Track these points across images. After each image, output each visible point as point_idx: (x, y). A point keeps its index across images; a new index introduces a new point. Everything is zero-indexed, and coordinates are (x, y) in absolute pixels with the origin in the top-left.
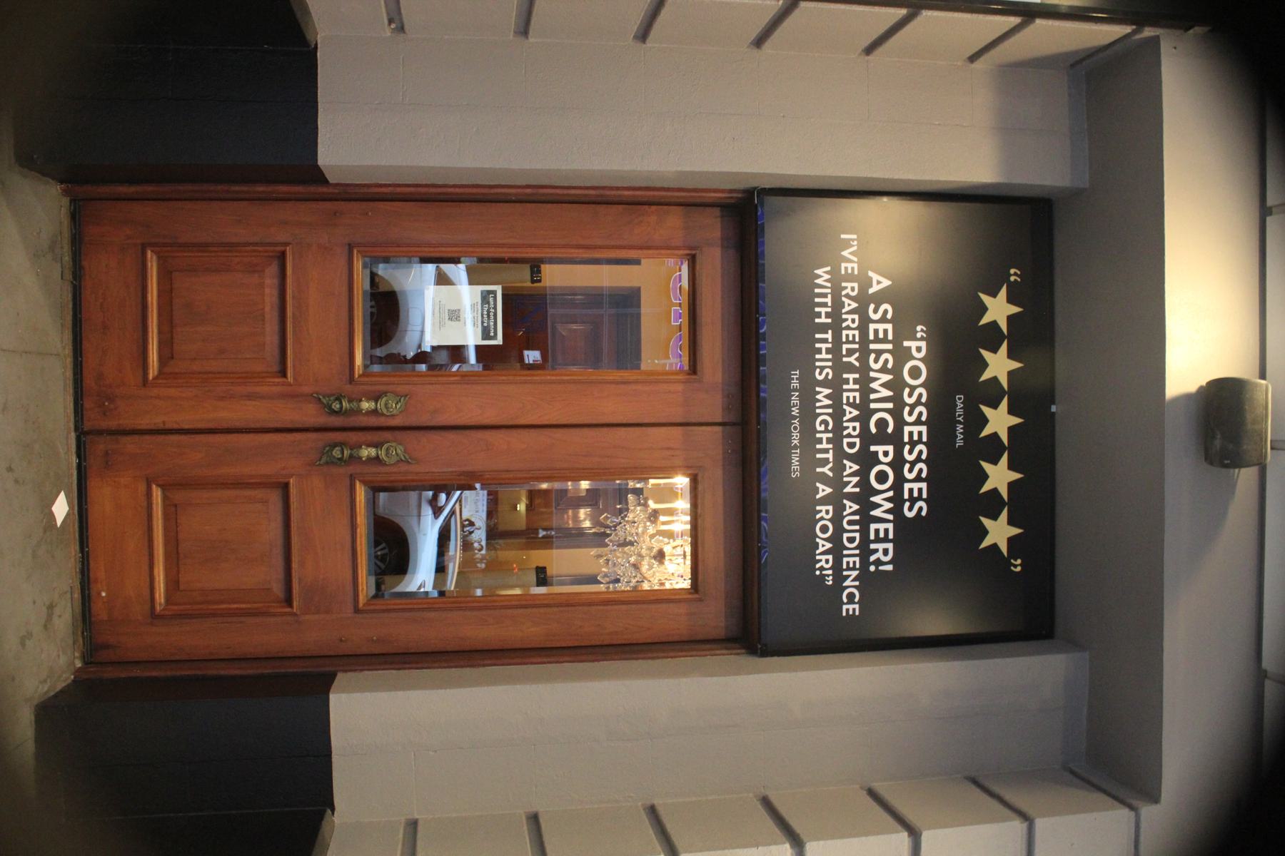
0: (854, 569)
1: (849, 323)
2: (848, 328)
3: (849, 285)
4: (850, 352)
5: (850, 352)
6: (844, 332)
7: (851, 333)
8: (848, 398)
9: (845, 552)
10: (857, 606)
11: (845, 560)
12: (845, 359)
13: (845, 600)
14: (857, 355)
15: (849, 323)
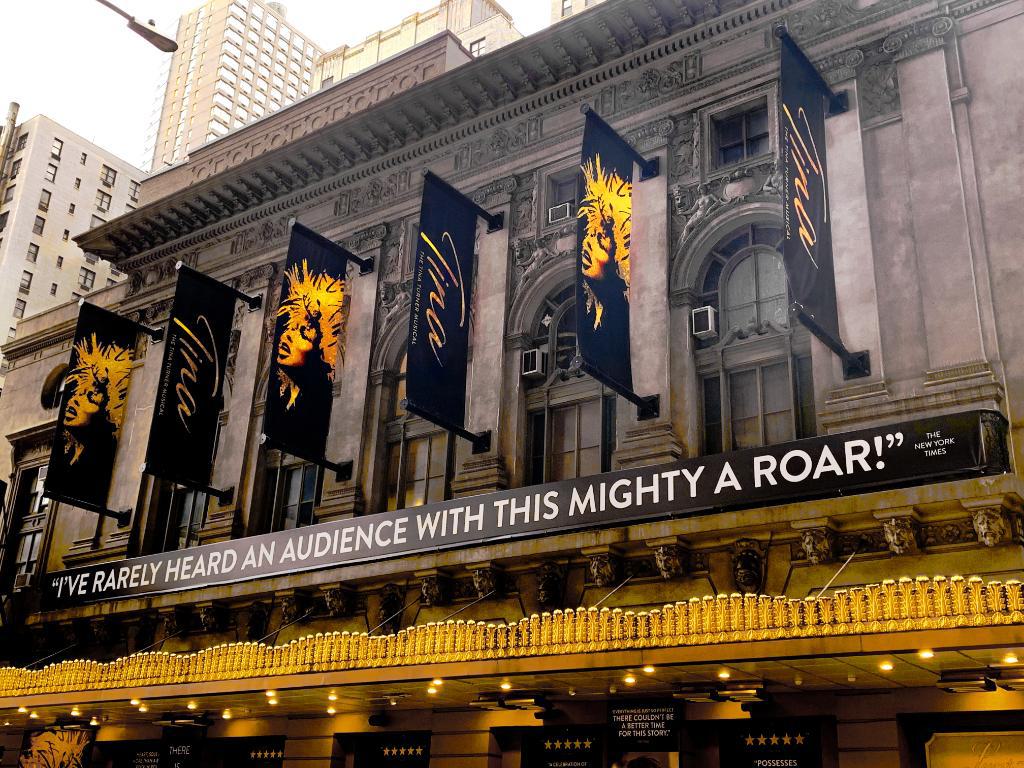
0: (353, 535)
3: (96, 582)
9: (334, 552)
10: (399, 521)
11: (343, 550)
12: (153, 582)
13: (389, 541)
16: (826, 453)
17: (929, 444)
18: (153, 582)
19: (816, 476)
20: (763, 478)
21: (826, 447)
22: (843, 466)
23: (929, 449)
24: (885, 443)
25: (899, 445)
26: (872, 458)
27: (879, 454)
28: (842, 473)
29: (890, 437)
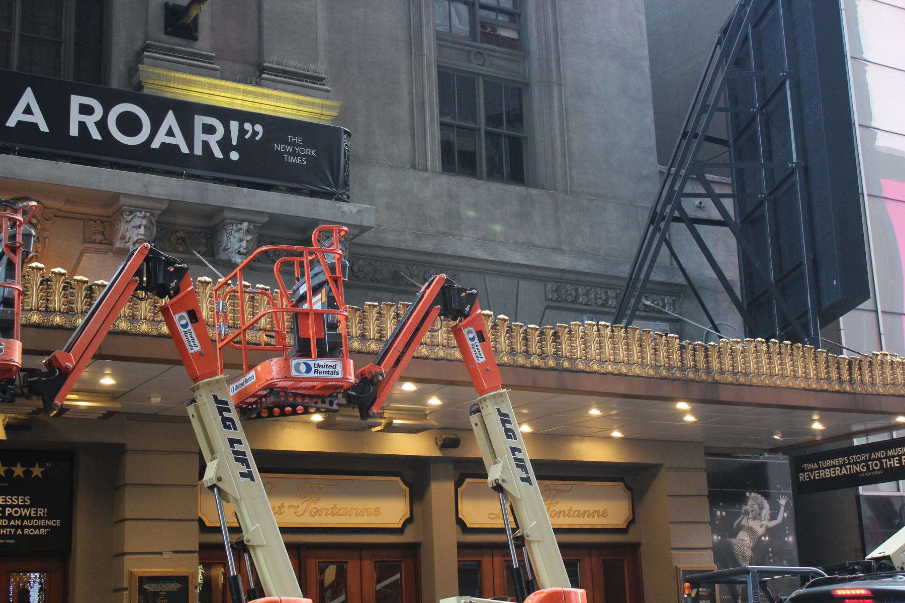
16: (170, 120)
17: (289, 149)
19: (155, 145)
20: (82, 126)
21: (171, 113)
22: (190, 142)
23: (288, 153)
24: (242, 132)
25: (257, 138)
26: (225, 144)
27: (234, 142)
28: (188, 152)
29: (248, 126)
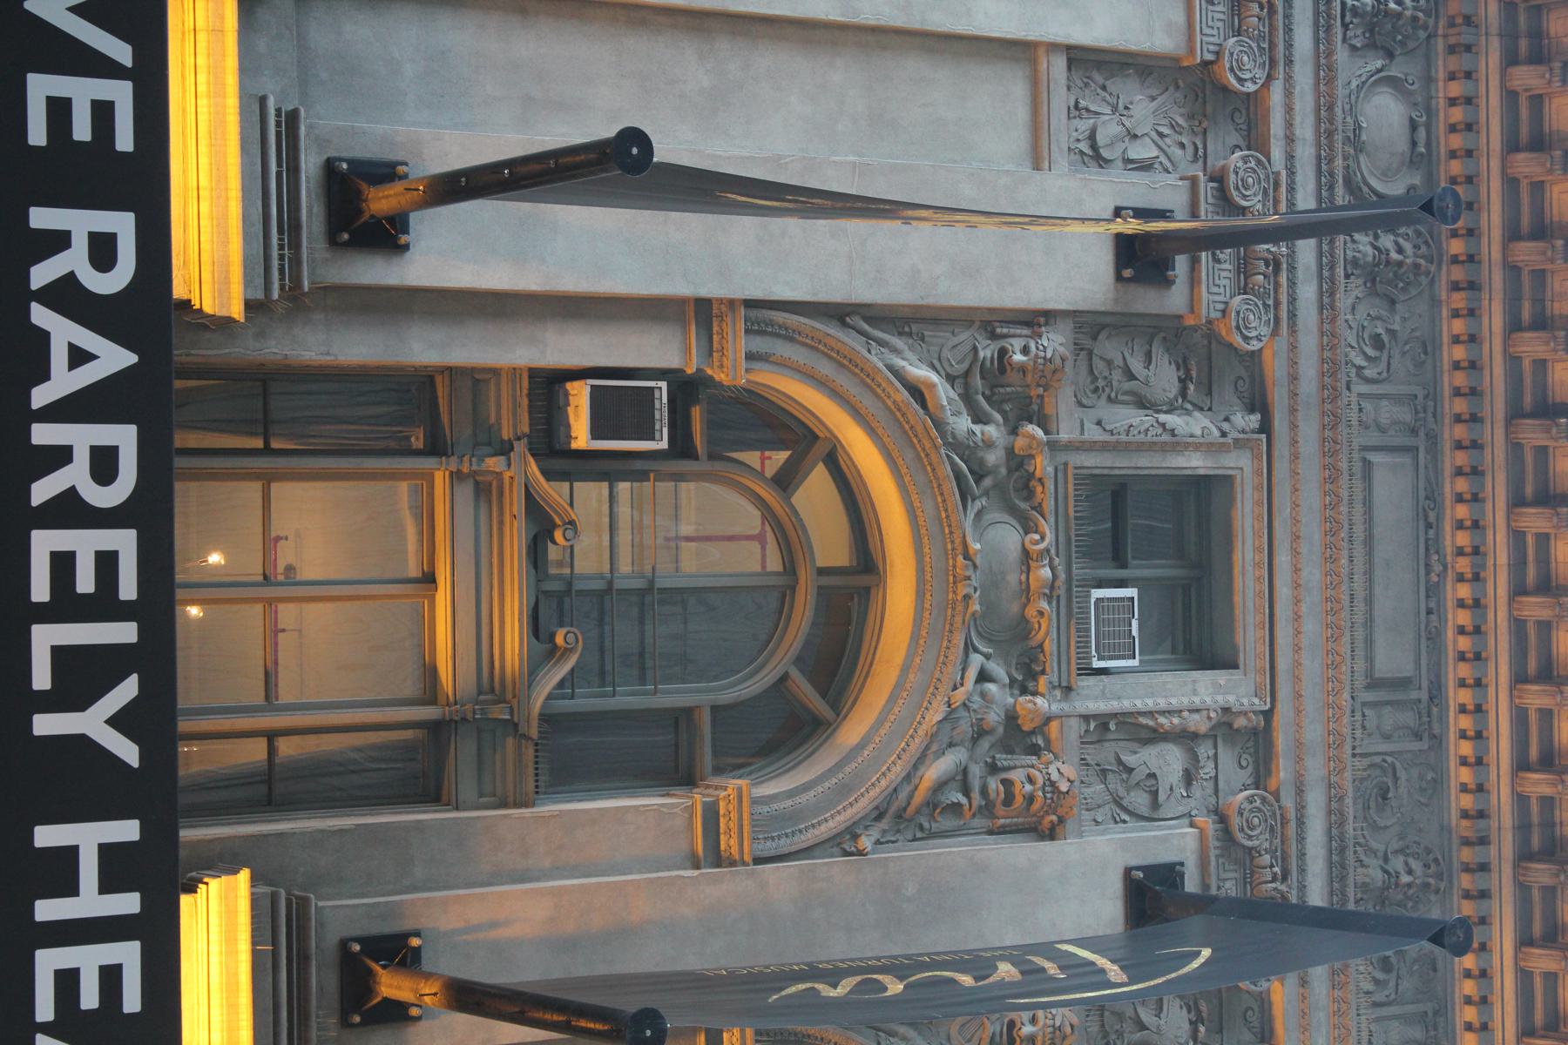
1: (76, 475)
2: (70, 512)
3: (80, 222)
4: (82, 676)
5: (82, 676)
6: (44, 543)
7: (85, 543)
8: (67, 981)
12: (46, 724)
14: (127, 690)
15: (76, 475)
18: (46, 724)
